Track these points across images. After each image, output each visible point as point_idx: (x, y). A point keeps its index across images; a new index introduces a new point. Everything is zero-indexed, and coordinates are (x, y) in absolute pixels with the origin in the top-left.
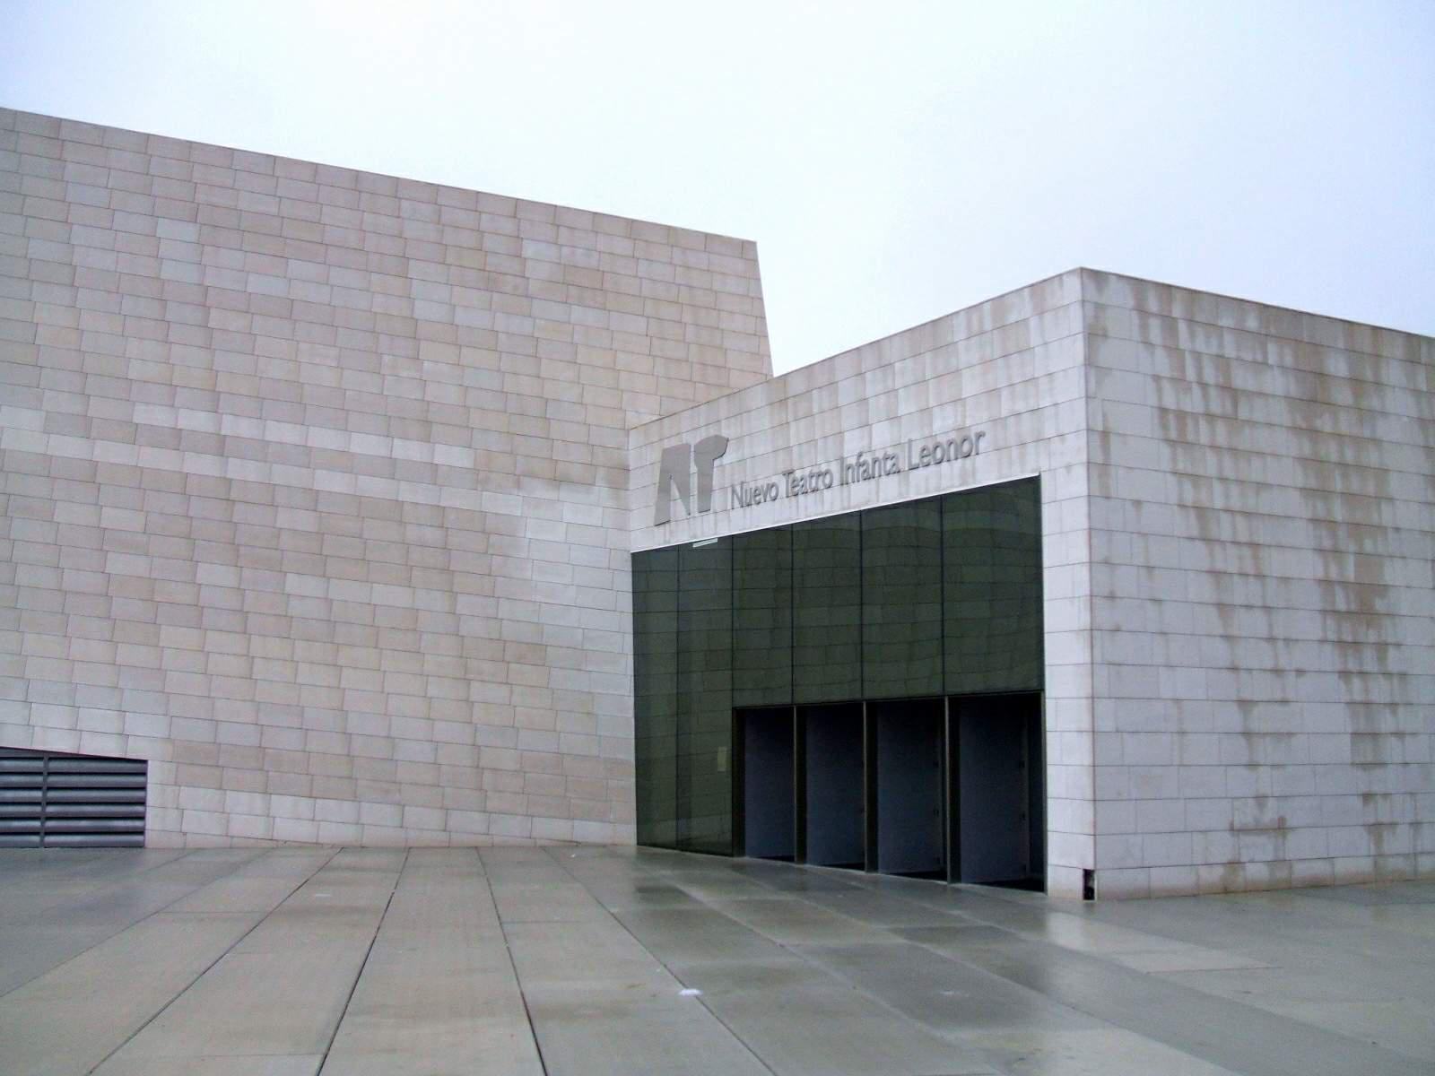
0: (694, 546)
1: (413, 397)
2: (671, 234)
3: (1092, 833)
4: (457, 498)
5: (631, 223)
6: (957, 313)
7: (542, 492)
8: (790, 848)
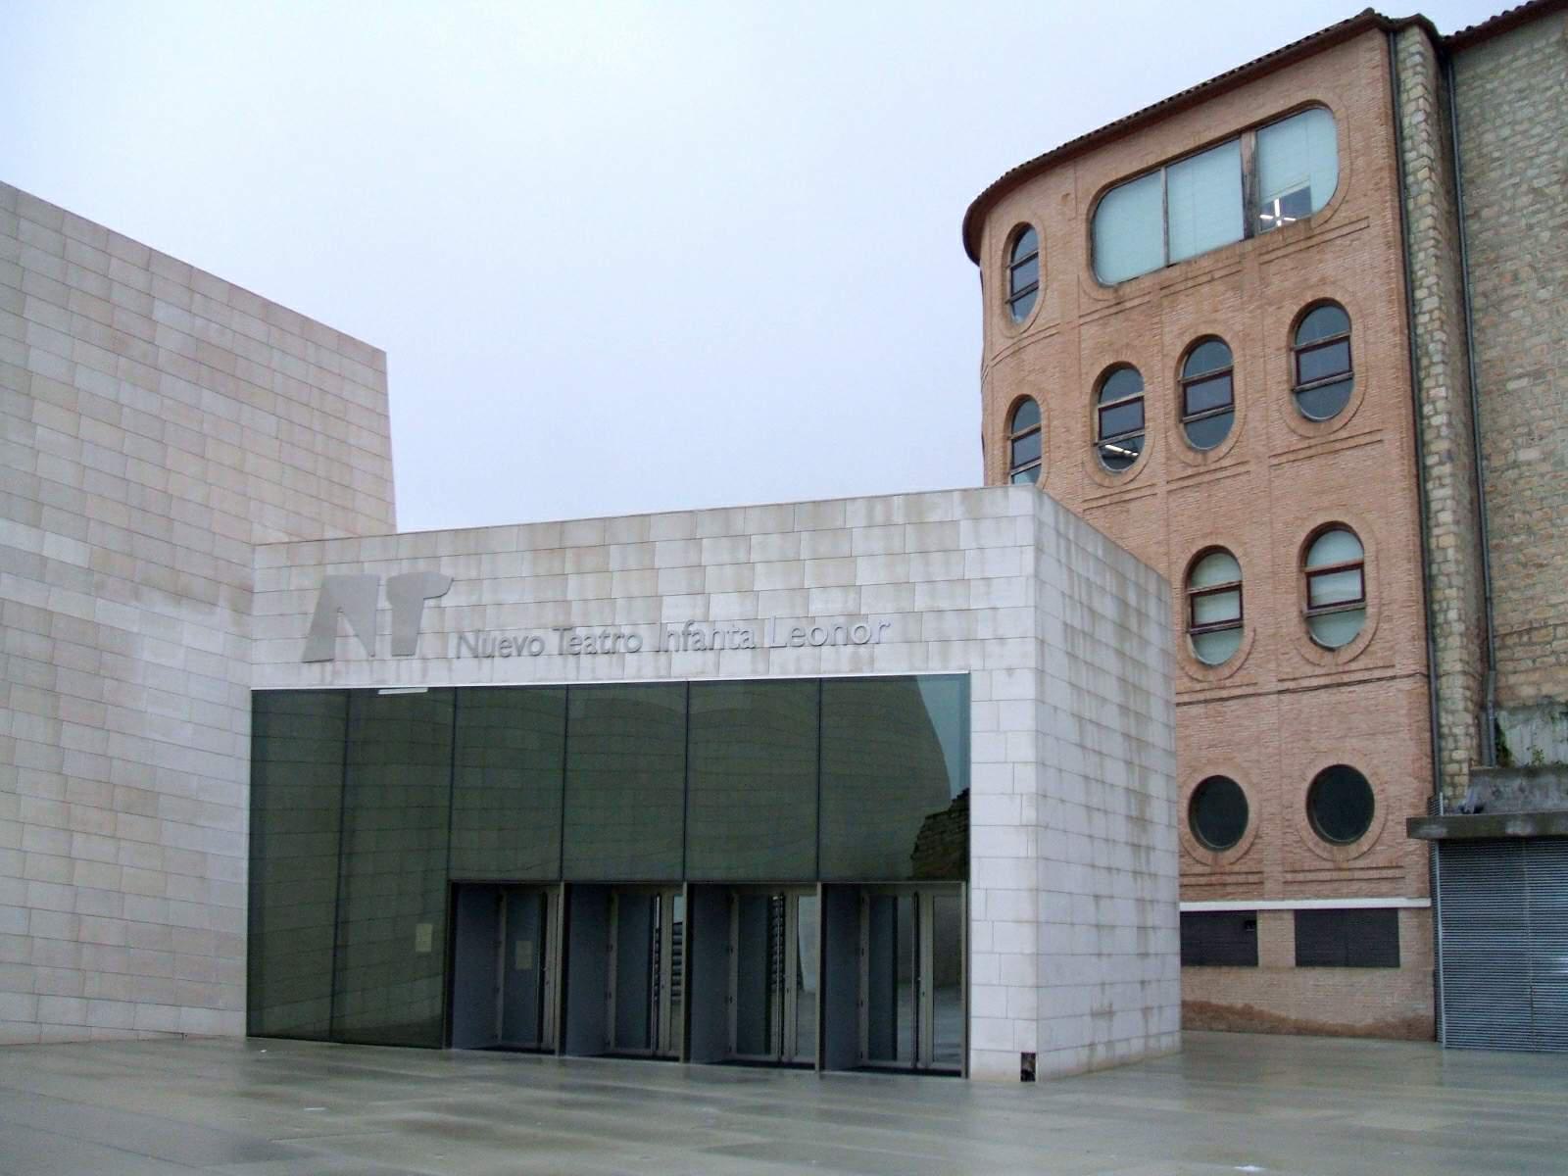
0: (381, 692)
1: (22, 469)
2: (306, 327)
3: (1035, 1017)
4: (69, 603)
5: (267, 305)
6: (854, 499)
7: (162, 606)
8: (514, 1036)
